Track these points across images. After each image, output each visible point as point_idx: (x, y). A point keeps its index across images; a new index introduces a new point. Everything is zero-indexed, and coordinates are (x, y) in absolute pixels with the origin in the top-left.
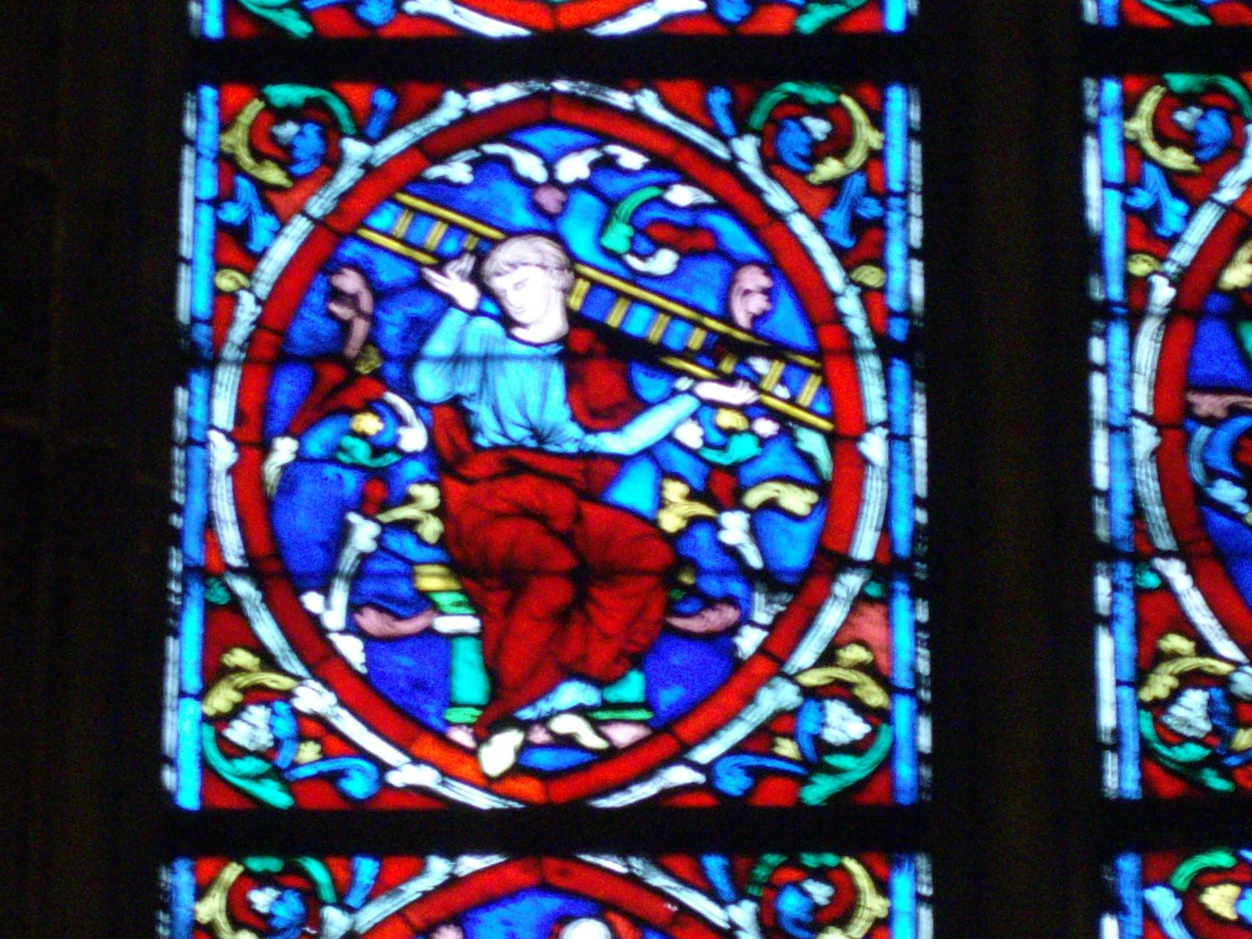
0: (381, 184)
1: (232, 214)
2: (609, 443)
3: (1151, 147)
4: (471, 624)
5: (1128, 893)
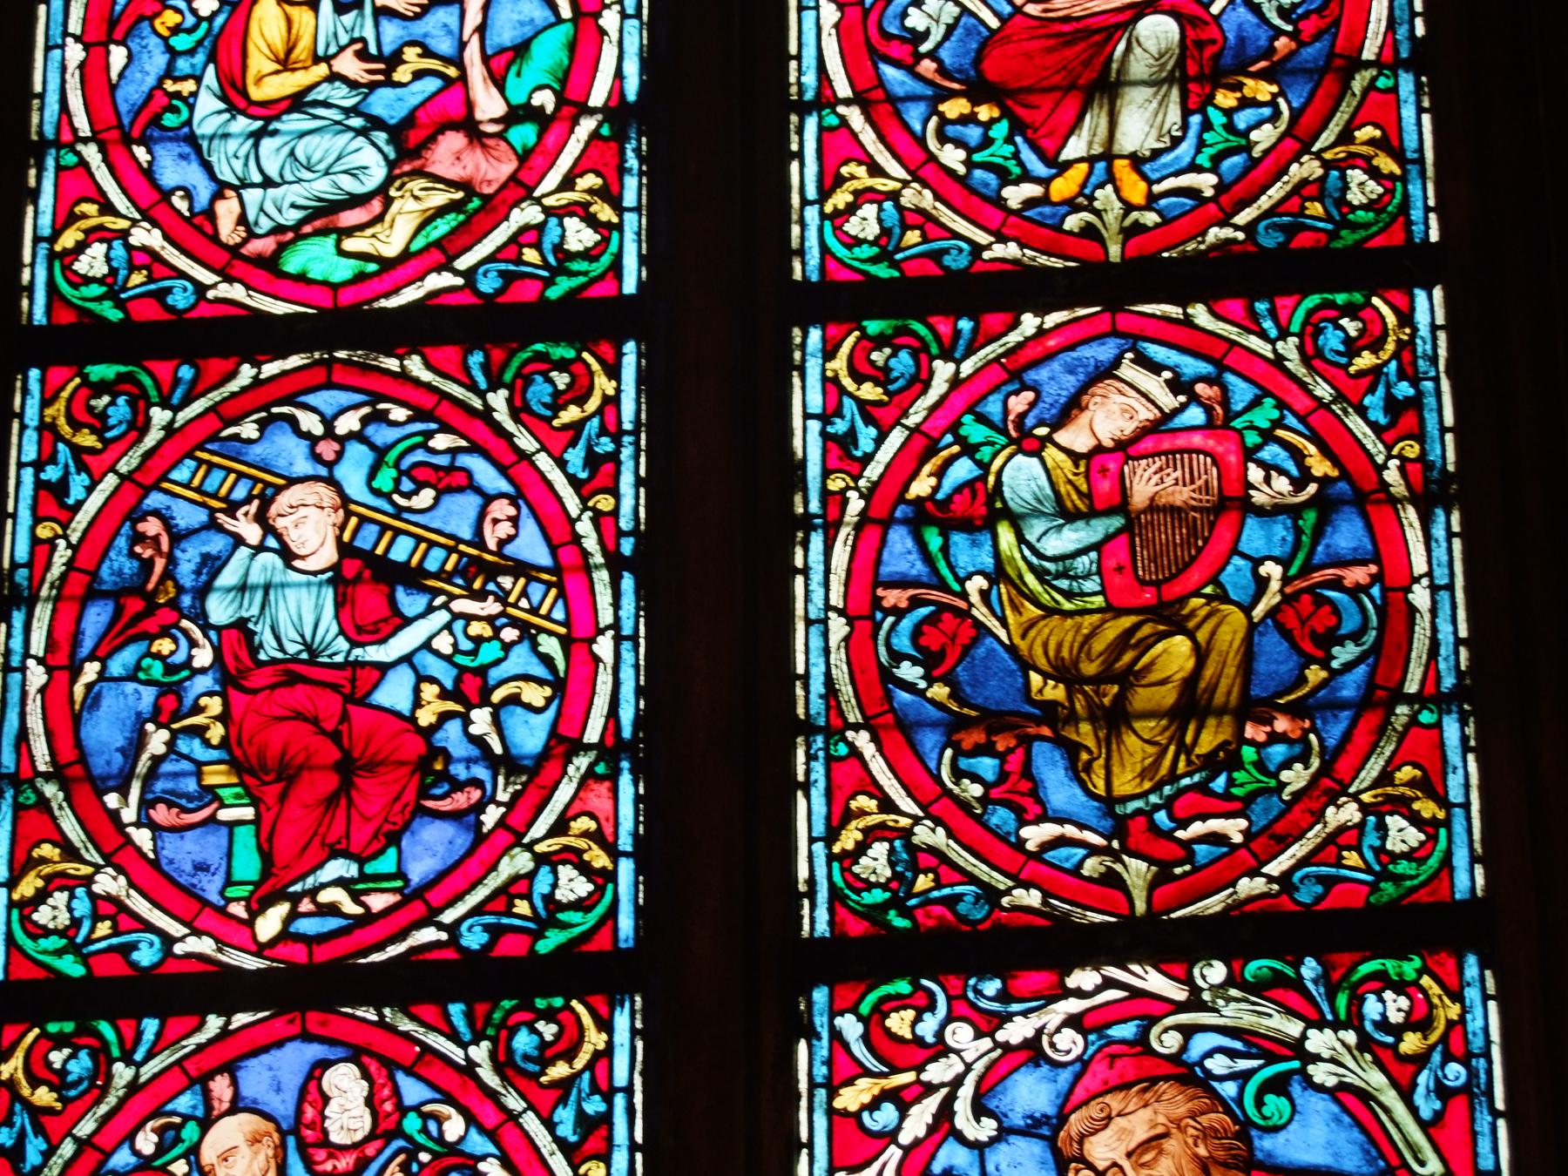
1: (52, 473)
2: (374, 653)
3: (847, 382)
4: (248, 813)
5: (820, 1022)
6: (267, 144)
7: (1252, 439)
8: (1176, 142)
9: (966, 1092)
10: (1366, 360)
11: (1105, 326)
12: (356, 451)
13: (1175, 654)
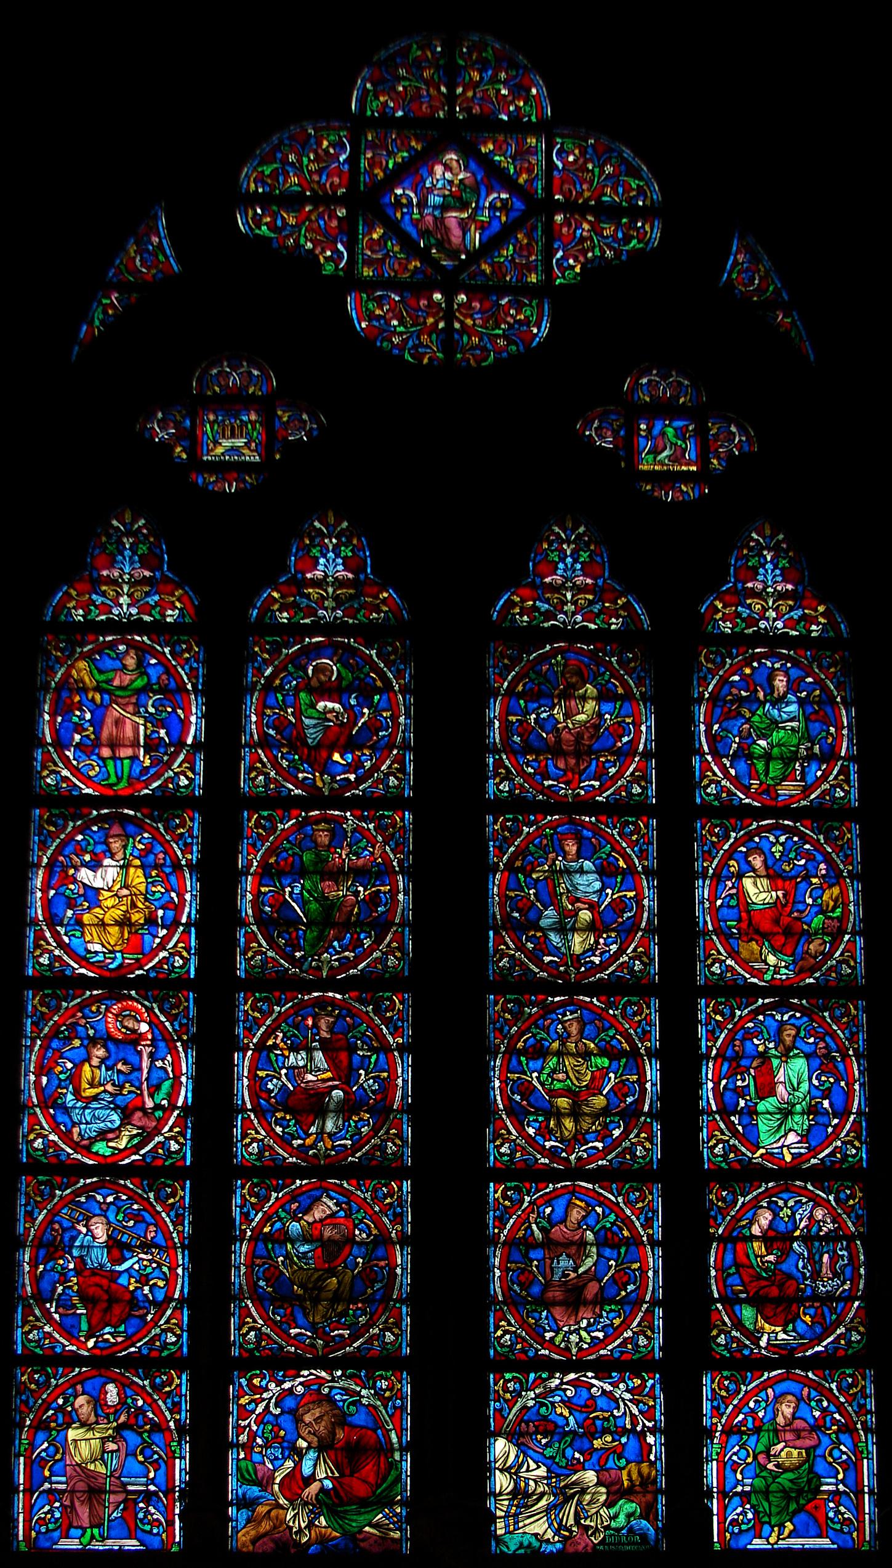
0: (65, 1202)
1: (29, 1208)
2: (118, 1268)
6: (87, 1111)
7: (357, 1222)
8: (341, 1130)
9: (273, 1401)
10: (388, 1201)
11: (318, 1185)
12: (112, 1207)
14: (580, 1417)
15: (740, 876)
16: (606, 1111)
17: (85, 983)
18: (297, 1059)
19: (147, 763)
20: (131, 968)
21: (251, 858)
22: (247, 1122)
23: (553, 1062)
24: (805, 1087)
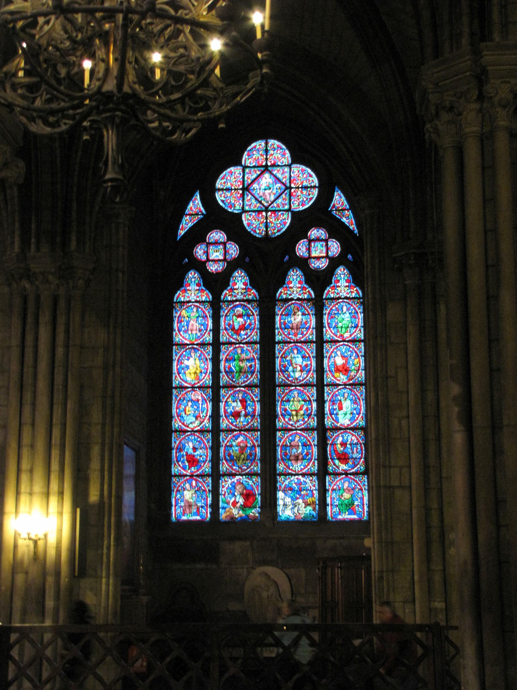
0: (183, 439)
13: (243, 456)
14: (298, 486)
15: (335, 357)
16: (304, 415)
17: (187, 388)
18: (234, 404)
19: (199, 335)
20: (197, 384)
21: (223, 357)
22: (223, 419)
23: (291, 403)
24: (350, 408)
